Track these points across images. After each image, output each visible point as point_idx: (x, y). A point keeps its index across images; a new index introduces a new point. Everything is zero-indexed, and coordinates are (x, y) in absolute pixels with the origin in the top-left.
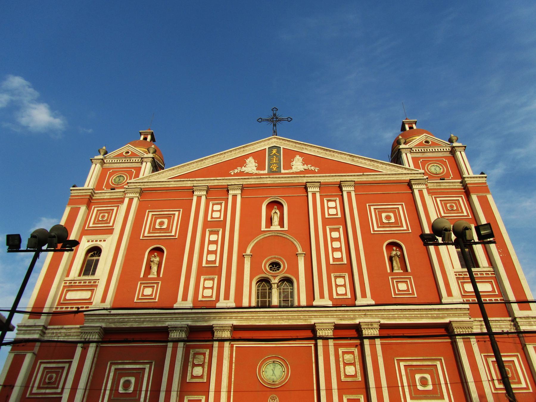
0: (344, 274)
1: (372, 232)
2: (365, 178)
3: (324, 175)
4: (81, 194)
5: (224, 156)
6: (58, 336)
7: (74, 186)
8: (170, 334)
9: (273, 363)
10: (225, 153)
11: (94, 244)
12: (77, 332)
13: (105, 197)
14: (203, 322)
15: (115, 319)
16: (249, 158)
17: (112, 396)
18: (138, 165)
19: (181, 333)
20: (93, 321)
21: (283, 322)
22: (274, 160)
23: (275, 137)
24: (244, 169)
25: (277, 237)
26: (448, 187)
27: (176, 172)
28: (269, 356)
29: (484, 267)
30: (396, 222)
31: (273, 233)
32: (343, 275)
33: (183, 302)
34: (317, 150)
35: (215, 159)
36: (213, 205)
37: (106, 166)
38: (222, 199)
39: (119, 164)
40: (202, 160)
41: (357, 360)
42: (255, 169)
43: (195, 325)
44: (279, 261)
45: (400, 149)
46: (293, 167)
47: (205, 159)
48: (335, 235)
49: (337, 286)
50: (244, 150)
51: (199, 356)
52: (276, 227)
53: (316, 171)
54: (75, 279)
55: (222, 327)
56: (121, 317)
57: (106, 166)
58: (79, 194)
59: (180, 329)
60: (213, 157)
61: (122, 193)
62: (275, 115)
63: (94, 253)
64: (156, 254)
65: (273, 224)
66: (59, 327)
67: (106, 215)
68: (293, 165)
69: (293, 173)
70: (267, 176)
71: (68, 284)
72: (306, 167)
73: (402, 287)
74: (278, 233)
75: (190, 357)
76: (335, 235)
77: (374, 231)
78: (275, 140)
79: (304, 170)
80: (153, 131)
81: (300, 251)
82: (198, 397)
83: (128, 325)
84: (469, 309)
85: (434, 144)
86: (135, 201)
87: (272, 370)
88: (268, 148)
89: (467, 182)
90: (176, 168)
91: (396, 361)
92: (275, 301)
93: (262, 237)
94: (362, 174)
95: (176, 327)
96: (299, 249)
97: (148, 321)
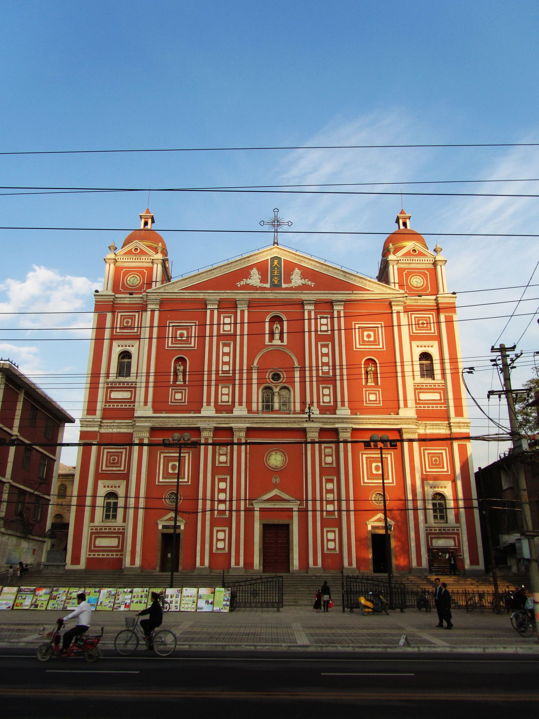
1: (354, 350)
3: (319, 292)
4: (105, 300)
11: (124, 348)
13: (126, 302)
16: (253, 269)
18: (150, 265)
20: (142, 422)
22: (276, 272)
24: (249, 281)
25: (278, 352)
26: (423, 304)
29: (437, 380)
30: (375, 341)
36: (224, 317)
37: (117, 264)
38: (231, 313)
41: (334, 453)
42: (259, 282)
45: (388, 261)
46: (293, 281)
48: (325, 350)
49: (324, 395)
52: (277, 342)
53: (313, 286)
55: (239, 429)
57: (118, 264)
58: (103, 300)
62: (276, 217)
63: (124, 355)
64: (180, 363)
65: (275, 338)
67: (130, 320)
68: (292, 279)
69: (291, 289)
70: (270, 292)
72: (303, 282)
73: (372, 397)
75: (217, 449)
76: (325, 350)
77: (356, 348)
79: (301, 285)
81: (296, 364)
85: (421, 254)
86: (157, 313)
88: (271, 258)
89: (439, 302)
91: (360, 454)
92: (276, 406)
94: (351, 292)
96: (295, 363)
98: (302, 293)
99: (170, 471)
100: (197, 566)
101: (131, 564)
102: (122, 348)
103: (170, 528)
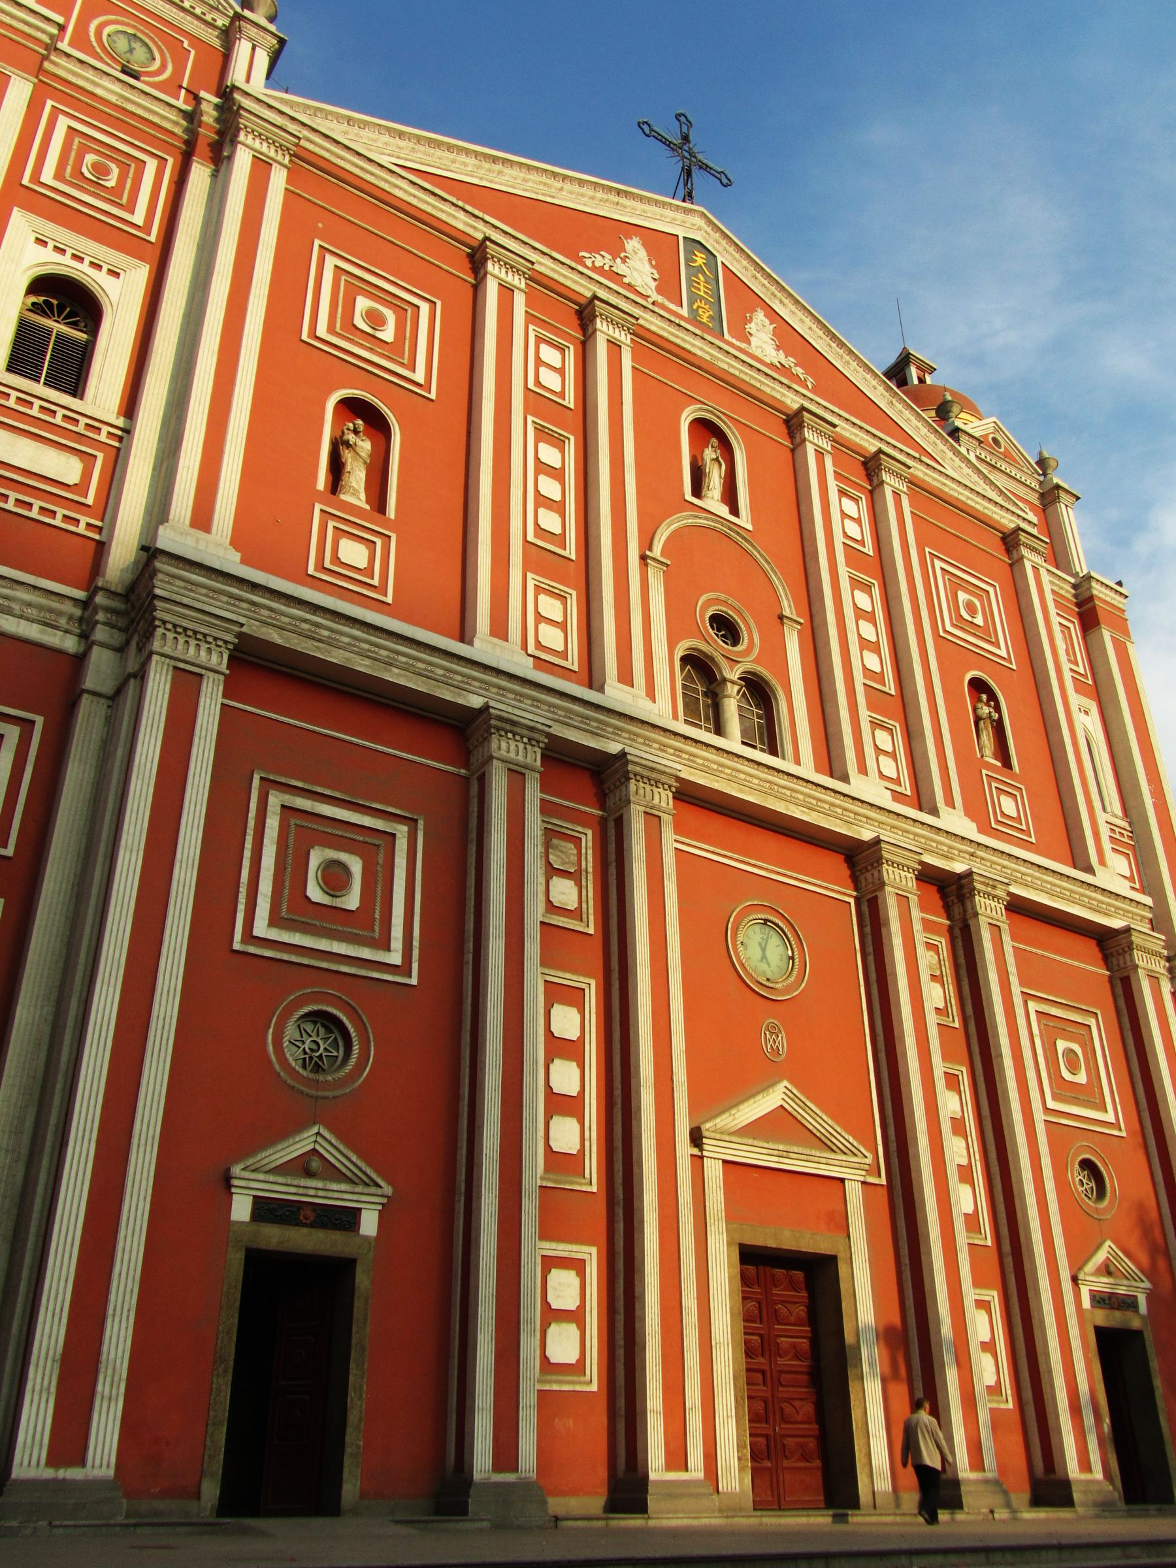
0: (890, 722)
2: (922, 471)
5: (561, 189)
10: (565, 178)
11: (64, 265)
12: (41, 608)
13: (99, 92)
14: (584, 733)
15: (283, 614)
17: (284, 907)
19: (529, 747)
23: (703, 215)
25: (727, 536)
27: (407, 148)
31: (716, 522)
33: (495, 640)
34: (808, 321)
40: (495, 160)
47: (505, 161)
50: (617, 204)
51: (563, 843)
55: (652, 769)
59: (525, 732)
60: (529, 168)
61: (175, 112)
62: (686, 138)
64: (359, 422)
74: (738, 533)
78: (701, 222)
82: (575, 978)
83: (336, 657)
84: (1150, 907)
87: (760, 944)
89: (1095, 592)
90: (410, 136)
93: (690, 521)
95: (514, 723)
96: (785, 604)
97: (405, 668)
98: (789, 387)
99: (315, 893)
100: (477, 1476)
101: (56, 1458)
102: (58, 258)
103: (299, 1224)
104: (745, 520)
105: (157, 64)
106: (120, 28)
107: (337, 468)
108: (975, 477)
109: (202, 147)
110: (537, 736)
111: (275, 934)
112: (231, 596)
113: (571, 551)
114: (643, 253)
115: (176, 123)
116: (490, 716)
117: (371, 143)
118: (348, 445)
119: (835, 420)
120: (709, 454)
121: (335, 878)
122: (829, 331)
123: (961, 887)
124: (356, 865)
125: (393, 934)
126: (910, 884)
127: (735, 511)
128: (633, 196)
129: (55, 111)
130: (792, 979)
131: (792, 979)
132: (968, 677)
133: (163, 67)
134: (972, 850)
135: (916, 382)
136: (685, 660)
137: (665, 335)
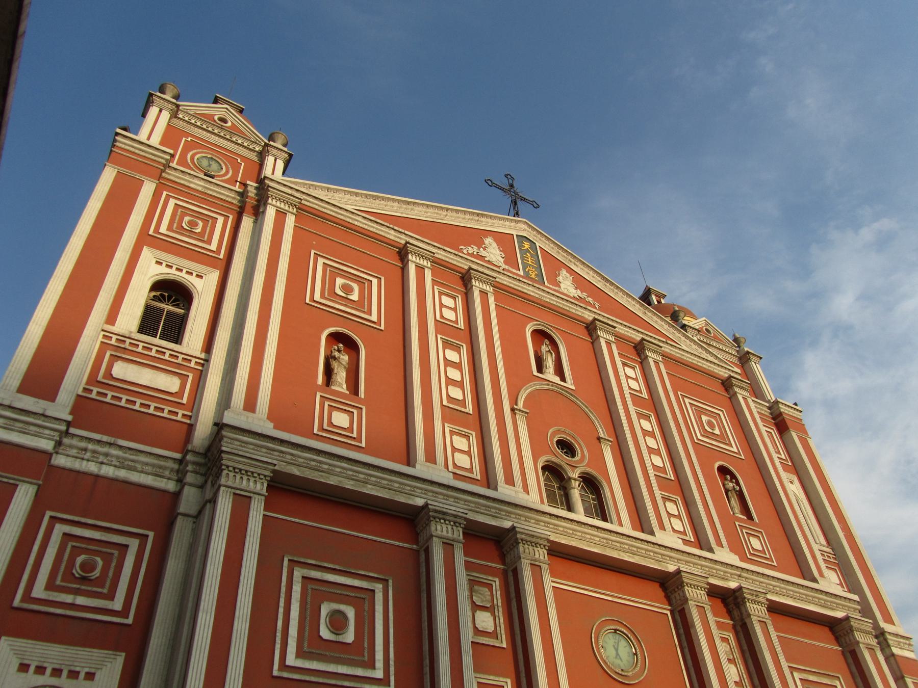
0: (674, 496)
2: (669, 349)
5: (446, 215)
6: (100, 460)
7: (125, 129)
8: (433, 523)
9: (614, 634)
10: (448, 209)
11: (172, 274)
12: (153, 466)
13: (192, 186)
17: (306, 644)
19: (454, 528)
21: (625, 556)
25: (561, 393)
28: (608, 618)
31: (553, 386)
32: (673, 499)
33: (428, 464)
35: (431, 213)
39: (209, 134)
40: (409, 203)
43: (473, 519)
44: (574, 442)
47: (414, 203)
50: (478, 220)
51: (481, 588)
54: (133, 336)
55: (532, 536)
56: (315, 457)
59: (451, 518)
60: (428, 206)
62: (512, 186)
64: (341, 345)
66: (105, 438)
71: (113, 342)
74: (566, 392)
78: (525, 227)
80: (244, 107)
82: (497, 679)
83: (333, 481)
84: (858, 602)
87: (614, 646)
89: (782, 410)
90: (362, 195)
93: (538, 387)
95: (444, 513)
99: (325, 633)
102: (168, 270)
104: (570, 384)
105: (224, 170)
106: (204, 155)
107: (329, 372)
108: (700, 350)
109: (248, 208)
110: (458, 520)
111: (300, 663)
112: (268, 448)
113: (470, 409)
114: (494, 245)
115: (234, 198)
116: (429, 510)
117: (340, 199)
118: (335, 358)
119: (615, 325)
120: (544, 348)
121: (338, 622)
122: (604, 277)
123: (736, 598)
124: (350, 612)
125: (377, 657)
126: (704, 598)
127: (563, 379)
128: (487, 216)
129: (168, 197)
130: (637, 669)
131: (637, 669)
132: (716, 466)
133: (227, 172)
134: (739, 573)
135: (656, 303)
136: (544, 468)
137: (512, 286)
